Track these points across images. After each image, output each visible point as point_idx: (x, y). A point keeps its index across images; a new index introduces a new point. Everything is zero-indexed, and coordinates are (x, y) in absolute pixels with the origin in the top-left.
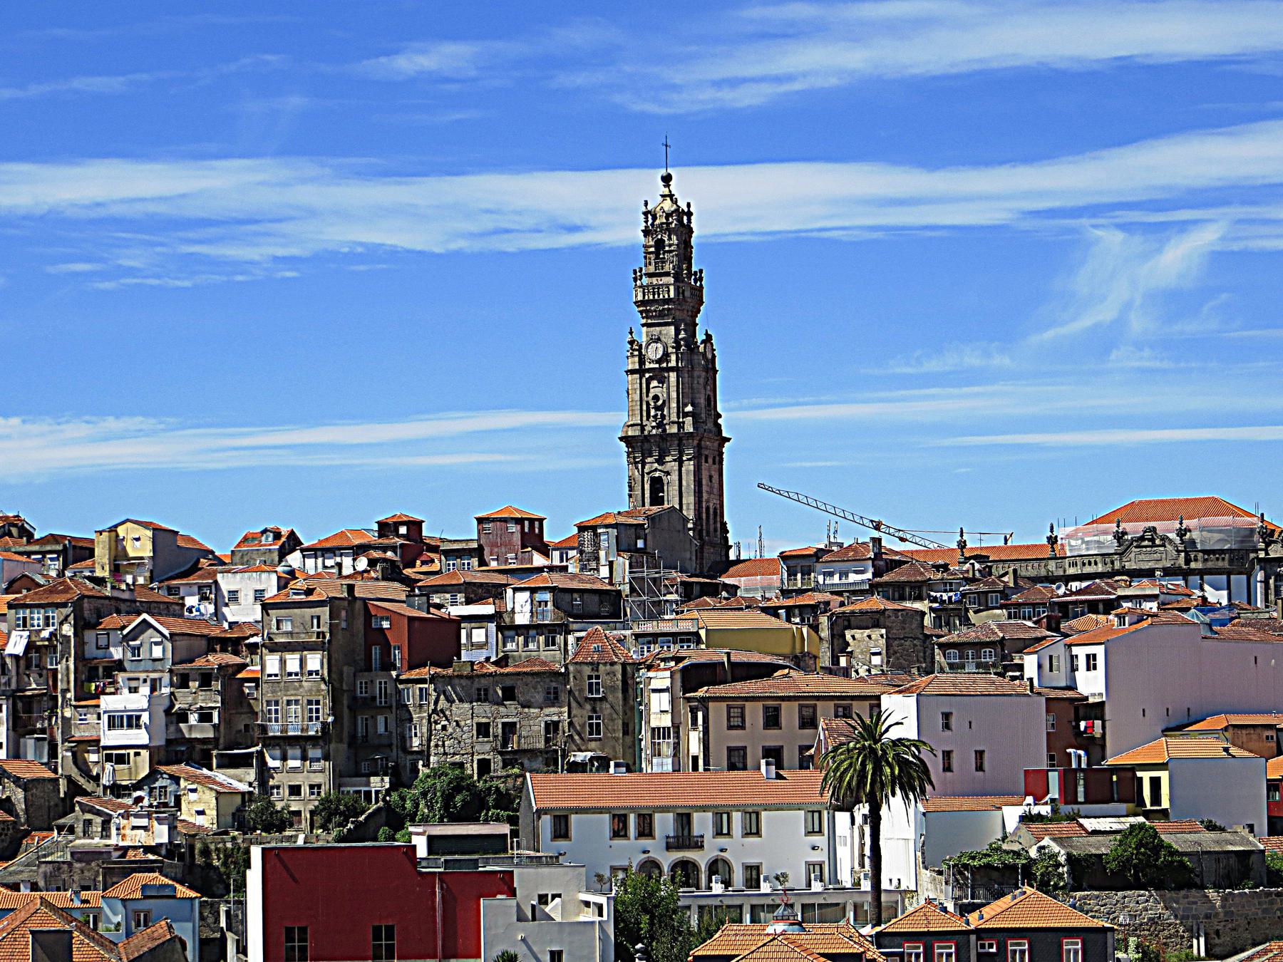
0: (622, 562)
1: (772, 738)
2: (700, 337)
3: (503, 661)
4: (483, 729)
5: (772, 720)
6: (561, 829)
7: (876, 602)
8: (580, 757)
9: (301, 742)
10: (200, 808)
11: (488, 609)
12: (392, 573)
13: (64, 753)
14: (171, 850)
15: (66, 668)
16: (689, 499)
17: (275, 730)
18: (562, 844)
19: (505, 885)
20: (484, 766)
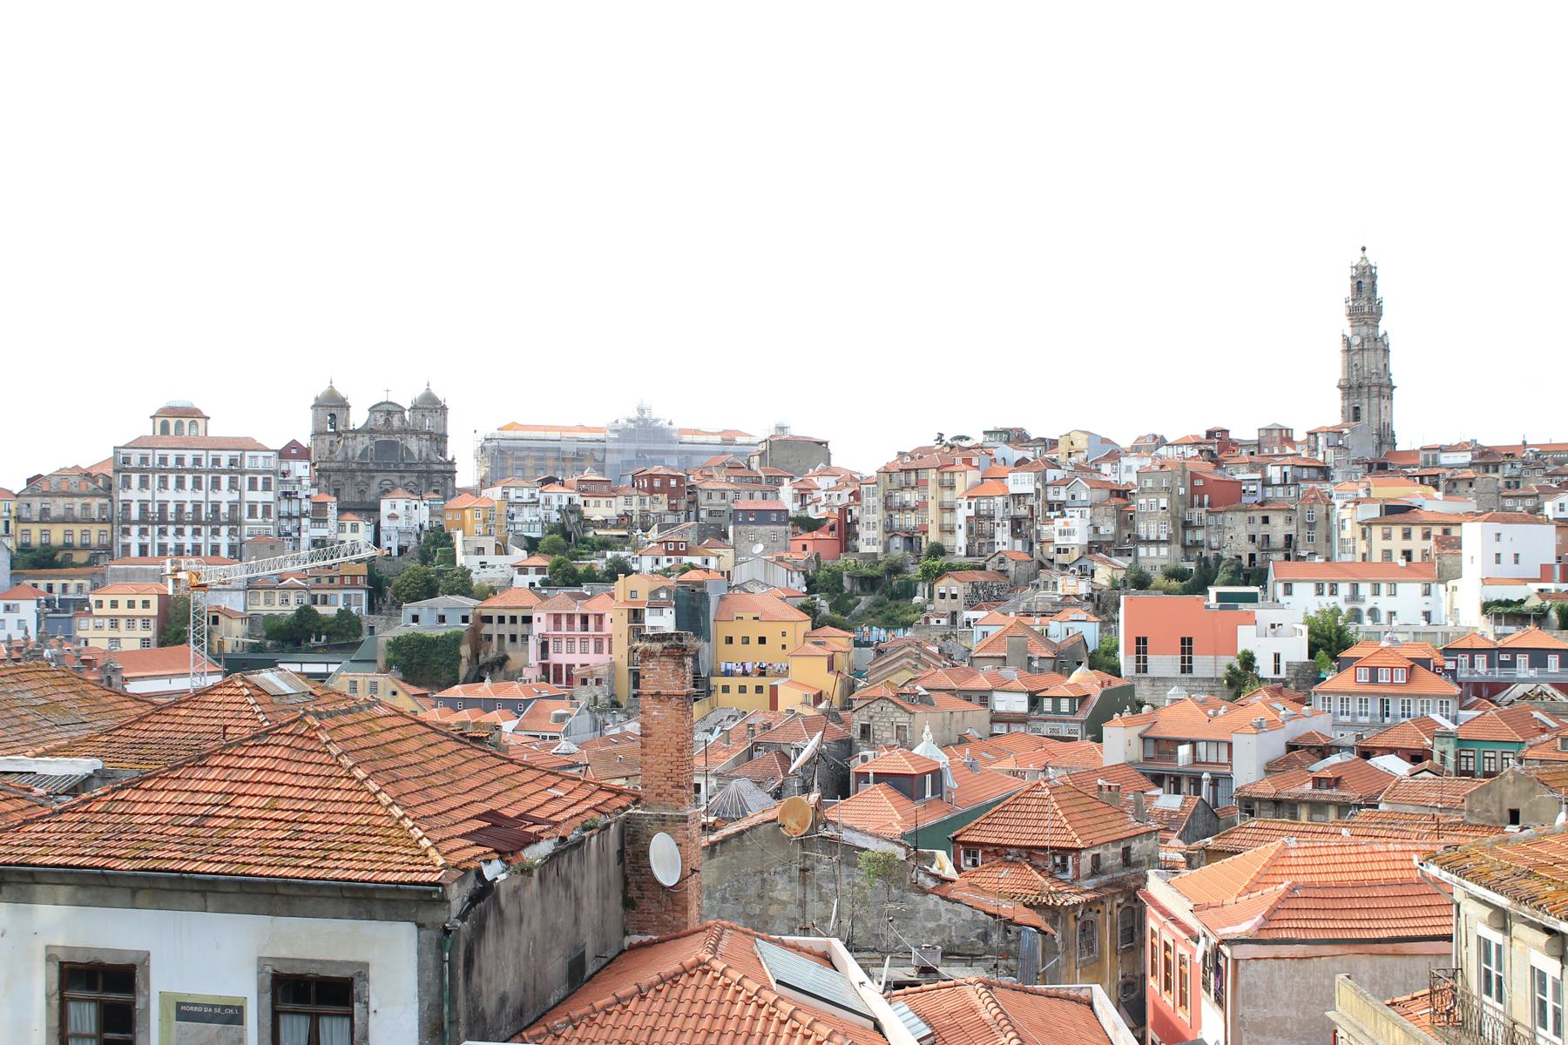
0: (1330, 452)
1: (1407, 545)
2: (1381, 333)
3: (1262, 504)
4: (1253, 538)
5: (1407, 536)
6: (1288, 590)
7: (1470, 473)
8: (1304, 553)
9: (1158, 542)
10: (1103, 576)
11: (1258, 476)
12: (1212, 458)
13: (1037, 547)
14: (1090, 598)
15: (1038, 505)
16: (1375, 419)
17: (1143, 536)
18: (1288, 598)
19: (1251, 620)
20: (1252, 557)
